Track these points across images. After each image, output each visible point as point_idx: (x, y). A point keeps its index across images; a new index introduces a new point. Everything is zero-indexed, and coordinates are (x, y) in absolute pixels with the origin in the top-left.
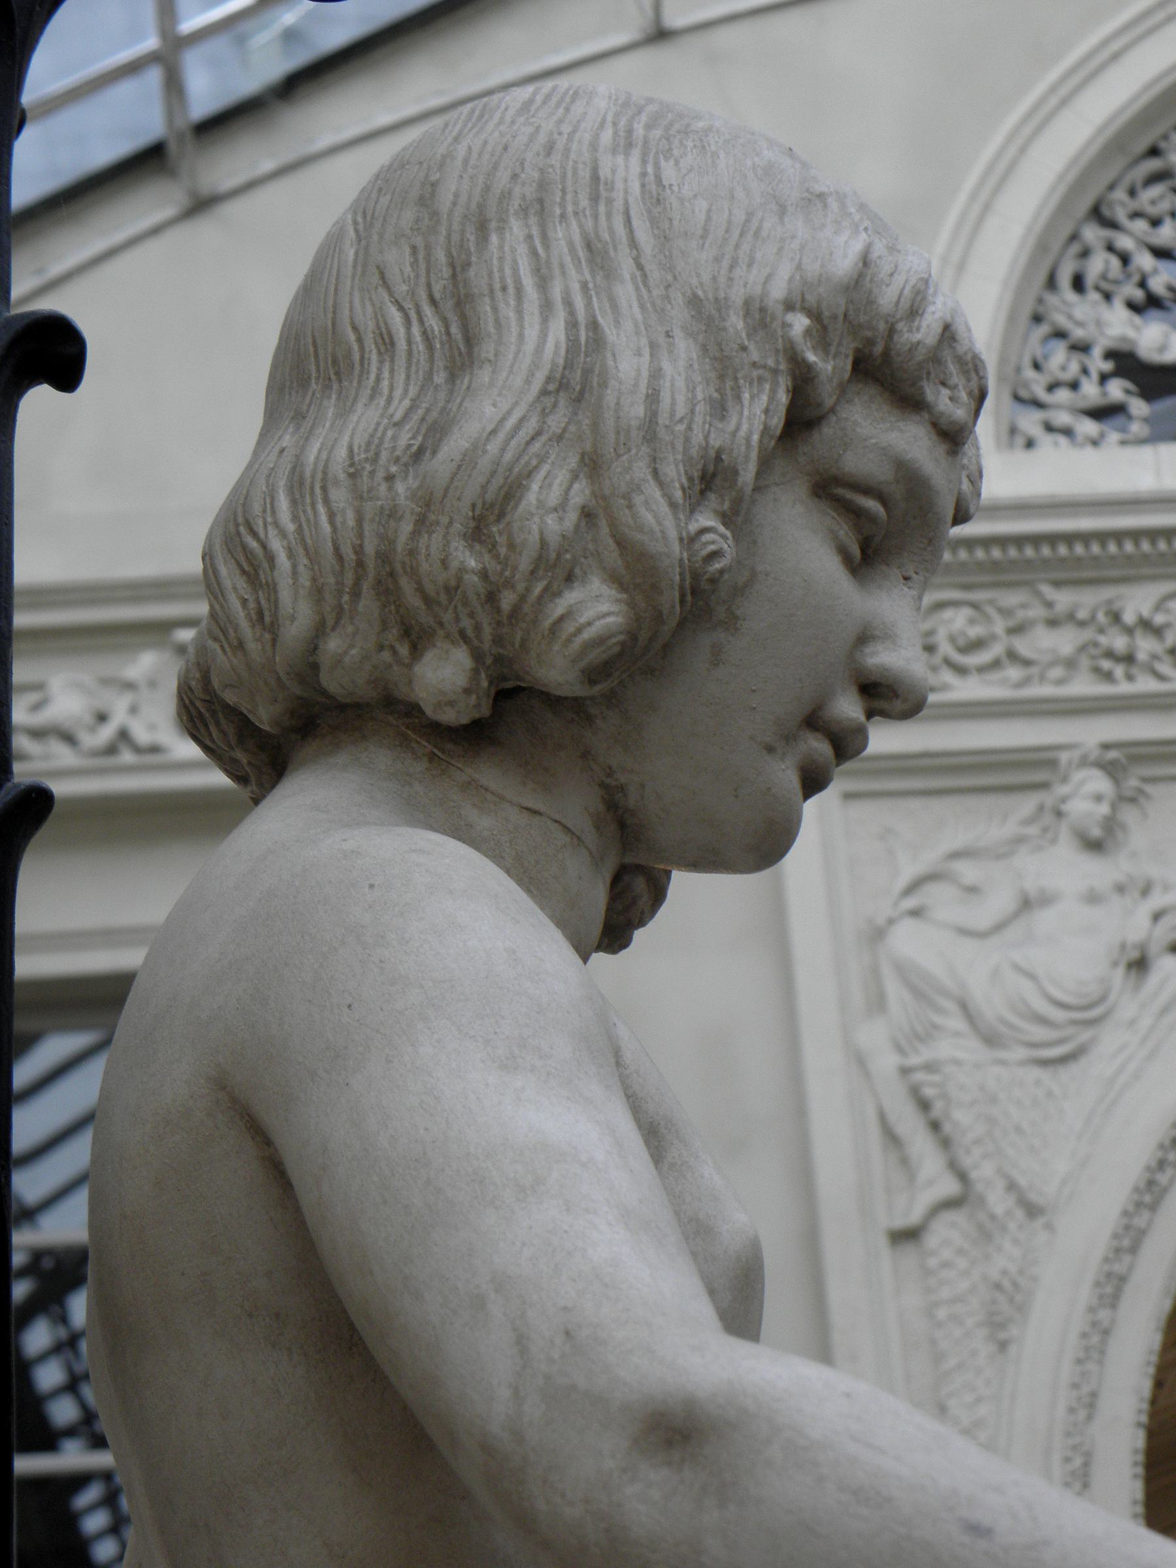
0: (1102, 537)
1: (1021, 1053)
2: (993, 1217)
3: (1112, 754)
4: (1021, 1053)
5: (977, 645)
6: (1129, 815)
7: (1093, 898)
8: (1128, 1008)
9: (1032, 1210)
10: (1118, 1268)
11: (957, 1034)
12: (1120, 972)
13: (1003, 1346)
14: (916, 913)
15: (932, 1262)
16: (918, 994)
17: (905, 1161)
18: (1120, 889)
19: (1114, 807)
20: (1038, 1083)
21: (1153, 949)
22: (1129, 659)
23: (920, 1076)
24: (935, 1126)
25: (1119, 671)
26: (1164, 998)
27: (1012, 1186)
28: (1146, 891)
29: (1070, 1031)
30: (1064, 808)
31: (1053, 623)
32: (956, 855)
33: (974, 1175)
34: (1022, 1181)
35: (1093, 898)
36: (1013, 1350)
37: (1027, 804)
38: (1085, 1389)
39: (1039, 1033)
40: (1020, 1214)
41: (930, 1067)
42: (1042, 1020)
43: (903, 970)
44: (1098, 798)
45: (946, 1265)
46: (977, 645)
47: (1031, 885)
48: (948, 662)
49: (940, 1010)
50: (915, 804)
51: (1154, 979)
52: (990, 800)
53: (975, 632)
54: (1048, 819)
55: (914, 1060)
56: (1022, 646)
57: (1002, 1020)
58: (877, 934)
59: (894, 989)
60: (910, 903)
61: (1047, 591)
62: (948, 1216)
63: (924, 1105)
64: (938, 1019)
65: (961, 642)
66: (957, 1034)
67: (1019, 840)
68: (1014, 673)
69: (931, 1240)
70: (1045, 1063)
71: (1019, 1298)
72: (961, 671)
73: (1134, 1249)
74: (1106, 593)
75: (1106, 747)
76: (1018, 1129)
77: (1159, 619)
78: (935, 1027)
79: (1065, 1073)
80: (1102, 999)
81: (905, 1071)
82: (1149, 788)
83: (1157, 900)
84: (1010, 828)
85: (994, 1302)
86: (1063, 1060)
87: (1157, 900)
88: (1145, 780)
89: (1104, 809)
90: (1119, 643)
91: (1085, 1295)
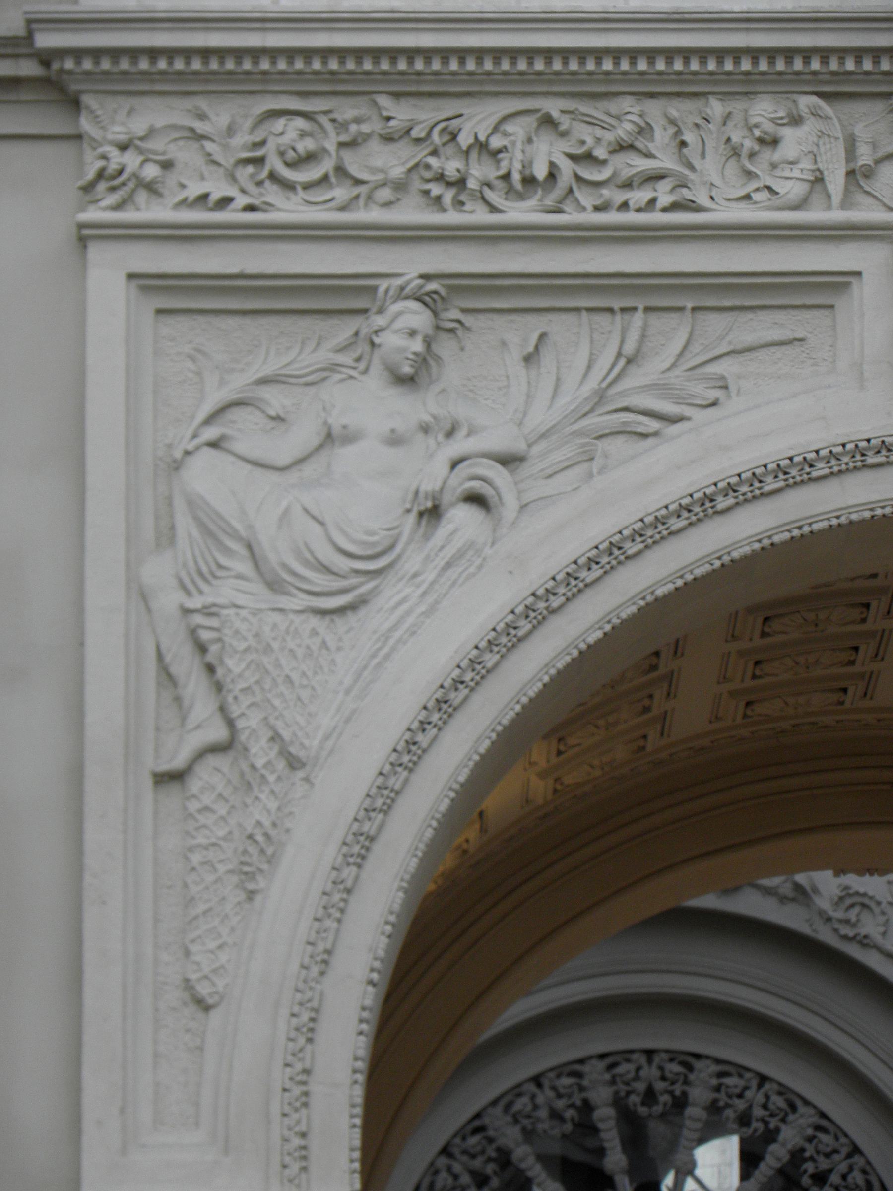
0: (445, 54)
1: (303, 601)
2: (253, 767)
3: (432, 286)
4: (303, 601)
5: (310, 158)
6: (445, 348)
7: (395, 440)
8: (412, 562)
9: (294, 763)
10: (366, 827)
11: (240, 577)
12: (412, 518)
13: (251, 895)
14: (214, 444)
15: (193, 806)
16: (207, 532)
17: (178, 699)
18: (425, 429)
19: (428, 343)
20: (314, 633)
21: (447, 498)
22: (460, 183)
23: (198, 619)
24: (211, 669)
25: (448, 196)
26: (449, 552)
27: (276, 737)
28: (450, 434)
29: (354, 581)
30: (377, 340)
31: (388, 139)
32: (264, 381)
33: (240, 724)
34: (286, 734)
35: (395, 440)
36: (258, 899)
37: (344, 329)
38: (321, 947)
39: (321, 581)
40: (281, 765)
41: (209, 611)
42: (327, 570)
43: (194, 504)
44: (413, 333)
45: (207, 809)
46: (310, 158)
47: (336, 421)
48: (273, 177)
49: (227, 552)
50: (232, 322)
51: (443, 530)
52: (305, 322)
53: (306, 145)
54: (362, 348)
55: (195, 603)
56: (354, 164)
57: (285, 566)
58: (177, 466)
59: (184, 524)
60: (211, 433)
61: (384, 101)
62: (213, 760)
63: (202, 648)
64: (223, 561)
65: (291, 155)
66: (240, 577)
67: (333, 368)
68: (341, 193)
69: (194, 785)
70: (323, 613)
71: (270, 851)
72: (288, 186)
73: (386, 810)
74: (449, 108)
75: (426, 277)
76: (288, 679)
77: (496, 142)
78: (220, 567)
79: (341, 624)
80: (392, 547)
81: (187, 612)
82: (468, 320)
83: (460, 446)
84: (324, 355)
85: (245, 852)
86: (341, 611)
87: (460, 446)
88: (465, 311)
89: (417, 346)
90: (452, 167)
91: (331, 853)
